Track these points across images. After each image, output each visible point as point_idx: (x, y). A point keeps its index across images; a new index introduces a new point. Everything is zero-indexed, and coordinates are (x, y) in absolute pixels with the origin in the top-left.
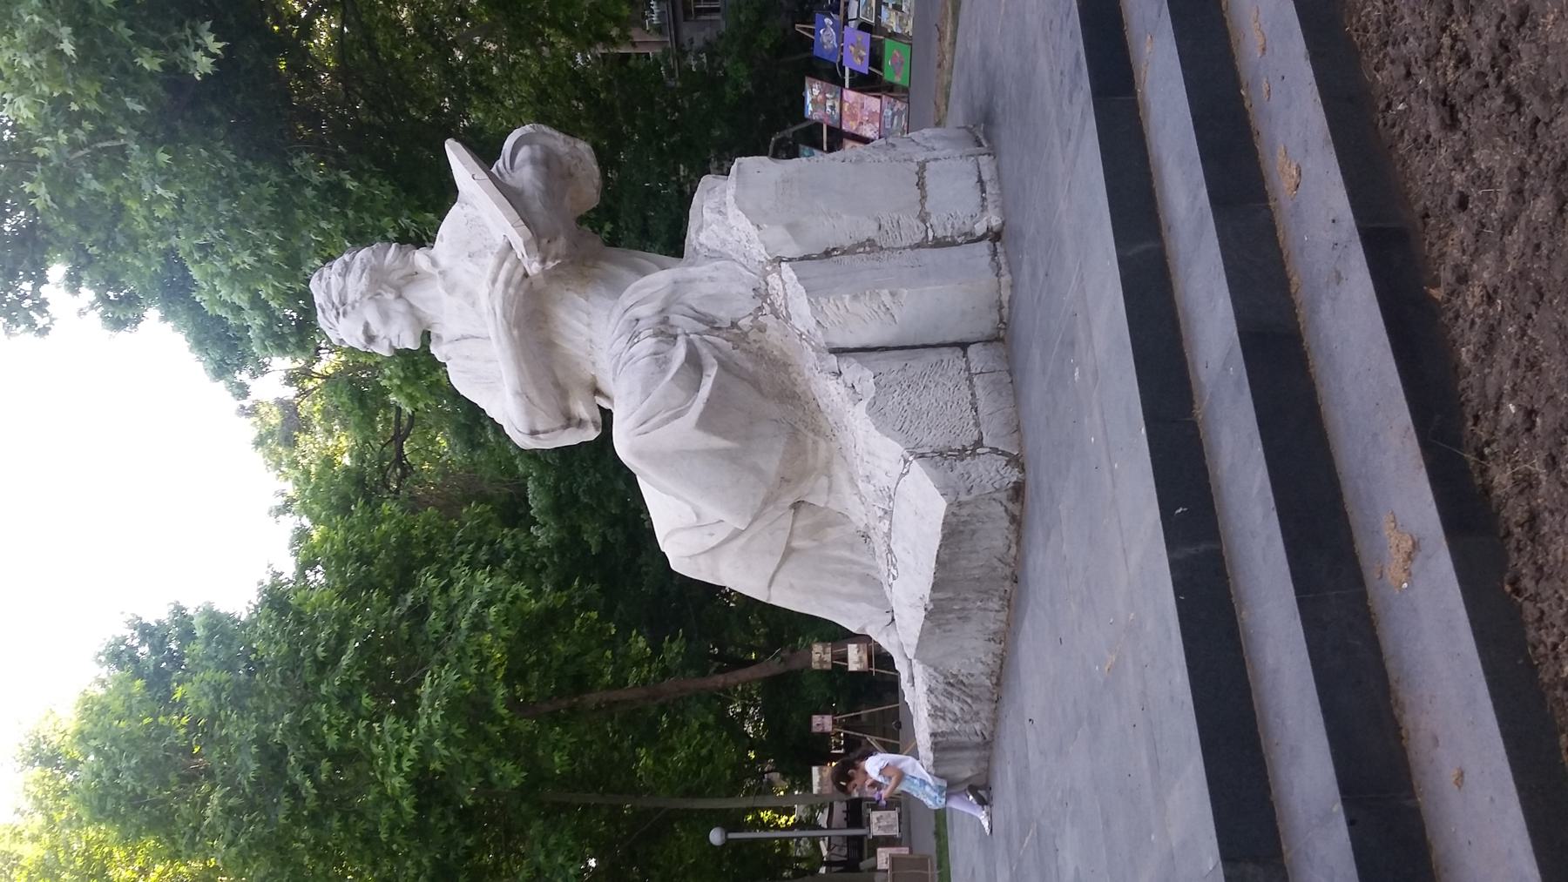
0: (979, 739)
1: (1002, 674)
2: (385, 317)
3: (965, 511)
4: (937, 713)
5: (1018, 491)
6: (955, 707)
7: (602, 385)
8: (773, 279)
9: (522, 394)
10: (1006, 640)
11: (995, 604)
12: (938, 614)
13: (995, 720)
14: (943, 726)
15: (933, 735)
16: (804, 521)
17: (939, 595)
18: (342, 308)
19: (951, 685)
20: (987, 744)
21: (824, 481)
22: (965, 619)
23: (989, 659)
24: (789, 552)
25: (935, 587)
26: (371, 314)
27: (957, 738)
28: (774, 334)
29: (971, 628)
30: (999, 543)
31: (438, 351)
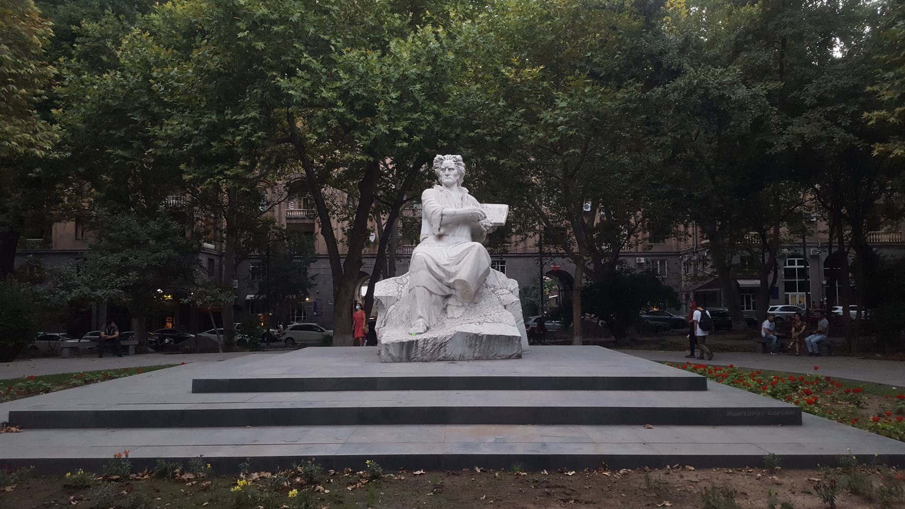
0: (412, 356)
1: (445, 359)
2: (455, 176)
3: (517, 342)
4: (426, 341)
5: (519, 357)
6: (429, 347)
7: (445, 238)
8: (506, 291)
9: (455, 214)
10: (462, 358)
11: (476, 355)
12: (477, 337)
13: (422, 361)
14: (420, 344)
15: (417, 341)
16: (439, 299)
17: (484, 338)
18: (456, 162)
19: (441, 345)
20: (409, 359)
21: (460, 304)
22: (470, 346)
23: (452, 356)
24: (431, 293)
25: (490, 337)
26: (455, 171)
27: (414, 348)
28: (485, 290)
29: (467, 349)
30: (502, 353)
31: (437, 187)
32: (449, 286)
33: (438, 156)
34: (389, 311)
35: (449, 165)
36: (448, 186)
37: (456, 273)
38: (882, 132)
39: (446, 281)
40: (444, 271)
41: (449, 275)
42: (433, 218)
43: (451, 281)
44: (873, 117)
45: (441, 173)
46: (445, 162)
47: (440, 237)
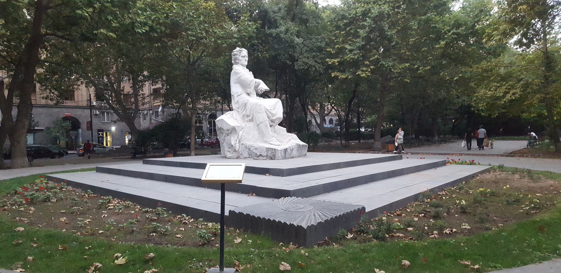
32: (272, 121)
33: (238, 49)
34: (241, 133)
35: (242, 55)
36: (243, 65)
37: (276, 114)
38: (332, 67)
39: (271, 118)
40: (270, 113)
41: (273, 115)
42: (252, 84)
43: (274, 118)
44: (330, 61)
45: (240, 58)
46: (243, 52)
47: (248, 94)
